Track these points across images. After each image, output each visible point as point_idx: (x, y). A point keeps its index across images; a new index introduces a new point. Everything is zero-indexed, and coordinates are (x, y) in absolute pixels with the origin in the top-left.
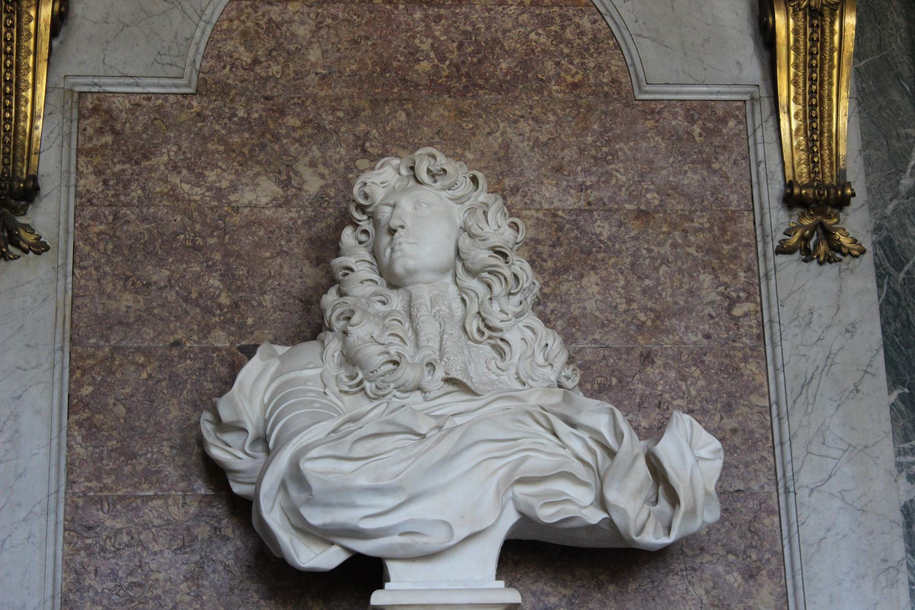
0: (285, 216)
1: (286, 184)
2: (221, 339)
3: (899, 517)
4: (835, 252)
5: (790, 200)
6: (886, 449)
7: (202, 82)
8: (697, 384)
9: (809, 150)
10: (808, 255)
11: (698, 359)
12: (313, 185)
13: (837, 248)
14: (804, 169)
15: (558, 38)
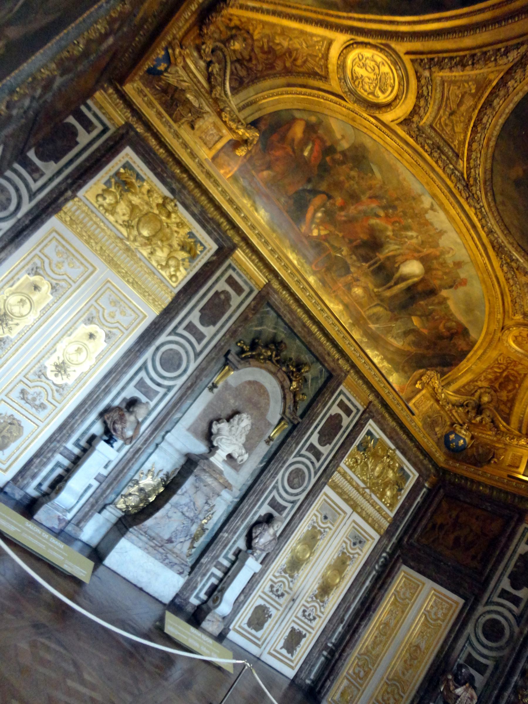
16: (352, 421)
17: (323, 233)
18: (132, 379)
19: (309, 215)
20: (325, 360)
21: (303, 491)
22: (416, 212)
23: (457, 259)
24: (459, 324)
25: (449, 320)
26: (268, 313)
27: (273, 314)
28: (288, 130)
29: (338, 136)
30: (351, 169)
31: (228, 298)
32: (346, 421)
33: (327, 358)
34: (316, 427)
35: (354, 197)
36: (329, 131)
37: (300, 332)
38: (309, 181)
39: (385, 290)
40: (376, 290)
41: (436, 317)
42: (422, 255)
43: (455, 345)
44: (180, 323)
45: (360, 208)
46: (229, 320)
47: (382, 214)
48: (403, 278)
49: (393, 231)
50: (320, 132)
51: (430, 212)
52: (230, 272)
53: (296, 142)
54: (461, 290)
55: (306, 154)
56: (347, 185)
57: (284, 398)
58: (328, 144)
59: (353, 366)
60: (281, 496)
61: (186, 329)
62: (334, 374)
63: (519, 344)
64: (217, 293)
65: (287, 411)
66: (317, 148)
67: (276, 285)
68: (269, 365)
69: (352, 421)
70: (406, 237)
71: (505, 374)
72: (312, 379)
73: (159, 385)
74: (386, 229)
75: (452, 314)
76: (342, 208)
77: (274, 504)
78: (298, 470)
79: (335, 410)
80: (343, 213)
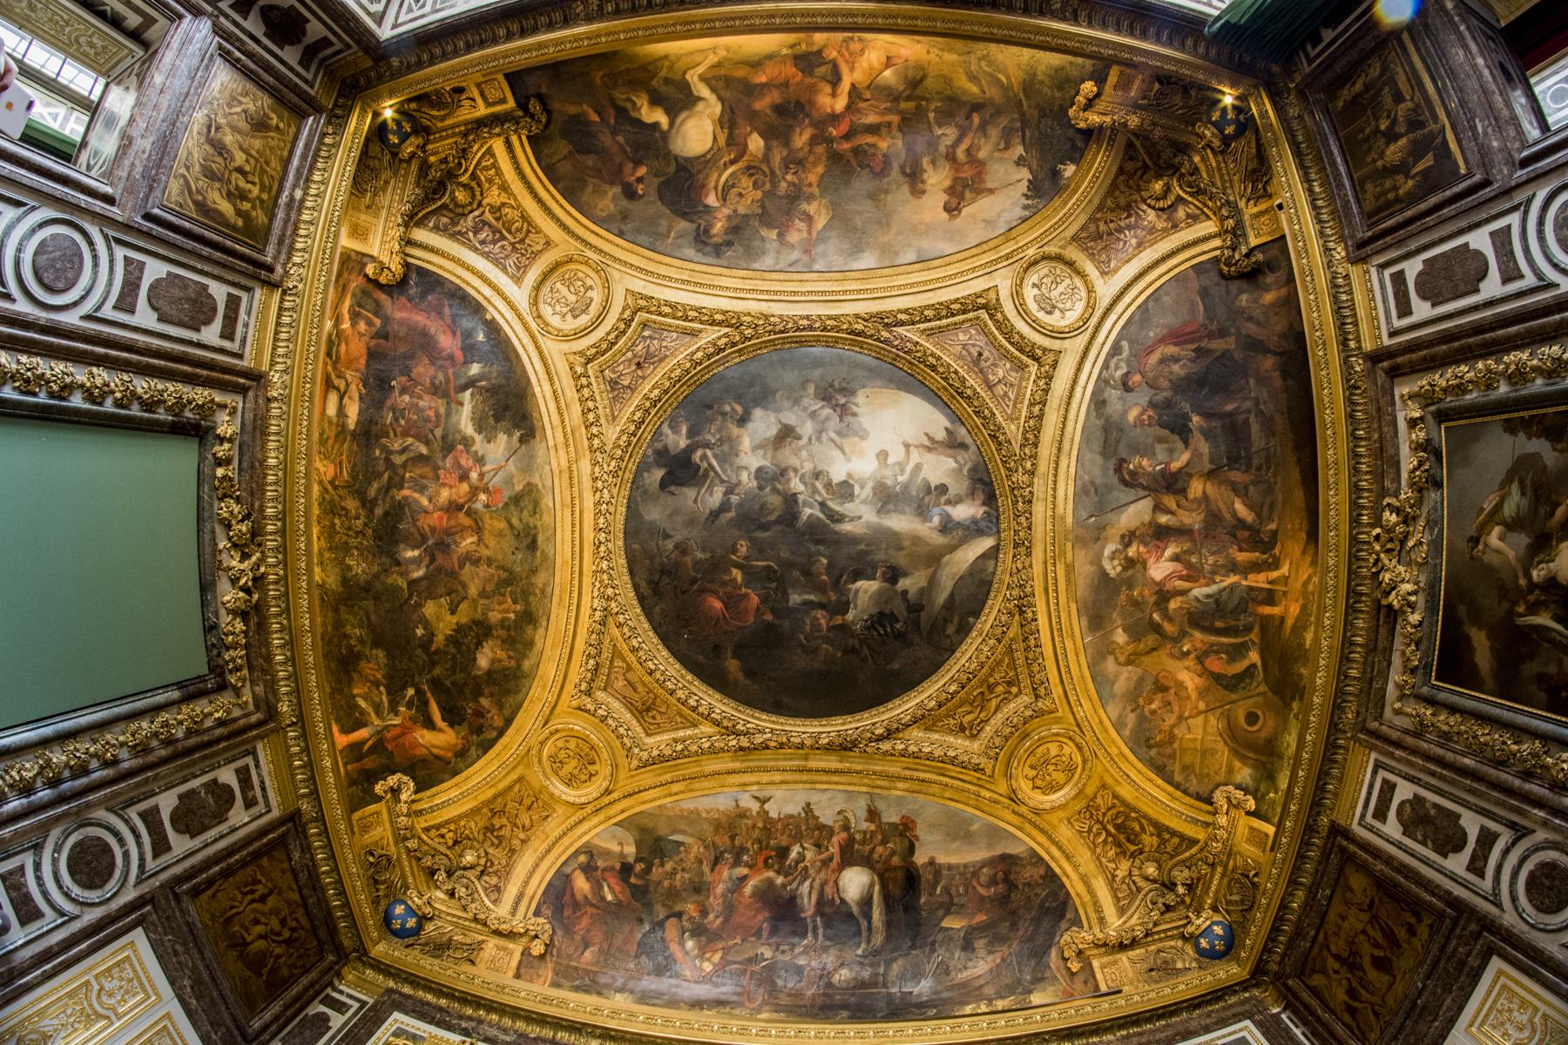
17: (717, 958)
19: (679, 955)
22: (760, 825)
23: (862, 814)
24: (991, 862)
25: (975, 874)
28: (573, 895)
29: (617, 849)
30: (662, 865)
35: (699, 888)
36: (607, 853)
38: (641, 921)
39: (869, 942)
40: (859, 952)
41: (961, 890)
42: (837, 859)
43: (1029, 884)
45: (720, 888)
47: (745, 871)
48: (866, 902)
49: (778, 872)
50: (600, 863)
51: (766, 806)
53: (590, 896)
54: (920, 831)
55: (609, 898)
56: (678, 884)
58: (618, 866)
63: (1053, 788)
66: (613, 881)
70: (797, 863)
71: (1110, 828)
74: (770, 882)
75: (966, 866)
76: (704, 913)
80: (711, 916)
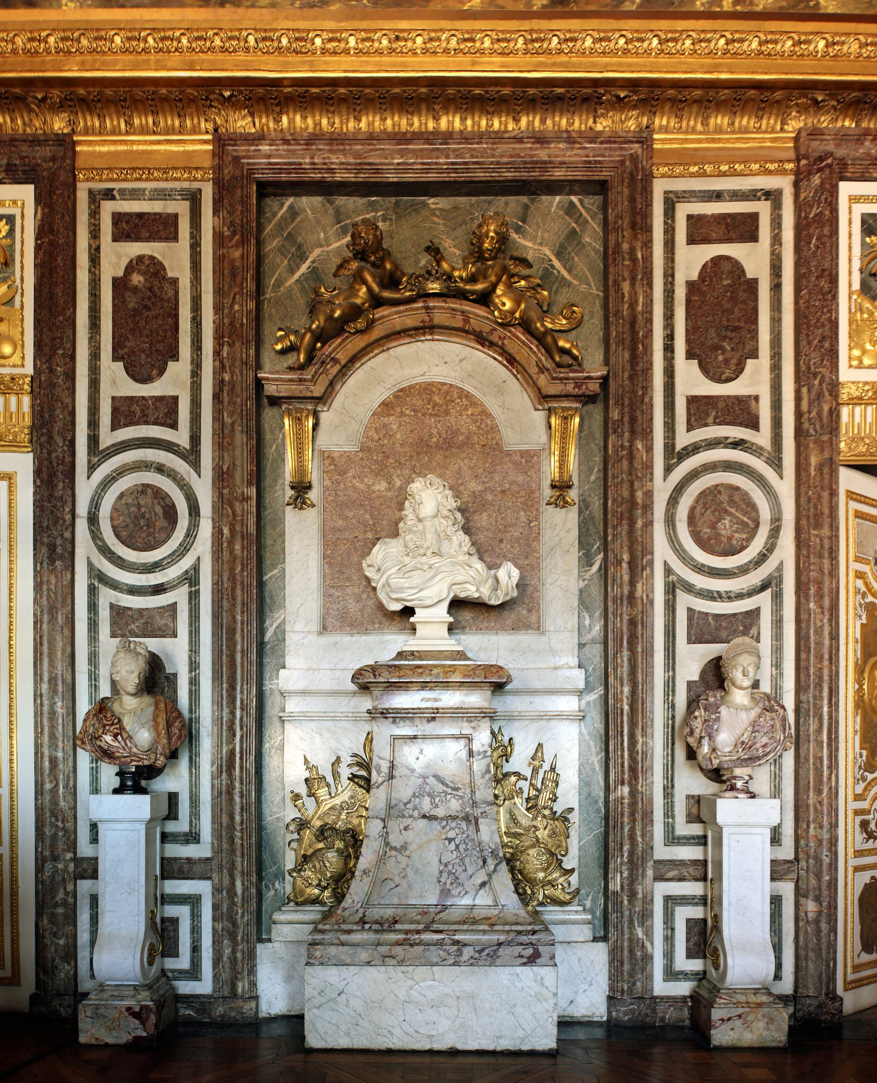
0: (389, 494)
1: (389, 483)
2: (370, 535)
3: (577, 592)
4: (566, 504)
5: (553, 487)
6: (576, 571)
7: (362, 447)
8: (517, 549)
9: (560, 468)
10: (557, 505)
11: (517, 541)
12: (398, 484)
13: (567, 503)
14: (557, 475)
15: (479, 427)
16: (777, 240)
18: (93, 626)
20: (544, 165)
21: (775, 532)
26: (293, 213)
27: (309, 203)
31: (153, 268)
32: (753, 259)
33: (542, 154)
34: (669, 349)
37: (403, 168)
44: (93, 423)
46: (198, 313)
52: (108, 208)
57: (511, 361)
59: (650, 95)
60: (712, 596)
61: (115, 425)
62: (605, 175)
64: (118, 284)
65: (543, 380)
67: (241, 123)
68: (391, 318)
69: (777, 240)
72: (558, 255)
73: (158, 590)
77: (703, 630)
78: (708, 496)
79: (692, 260)
